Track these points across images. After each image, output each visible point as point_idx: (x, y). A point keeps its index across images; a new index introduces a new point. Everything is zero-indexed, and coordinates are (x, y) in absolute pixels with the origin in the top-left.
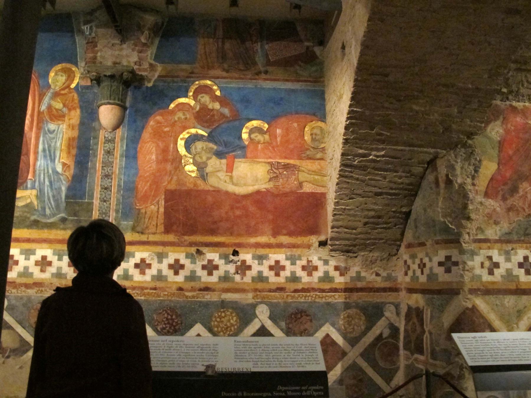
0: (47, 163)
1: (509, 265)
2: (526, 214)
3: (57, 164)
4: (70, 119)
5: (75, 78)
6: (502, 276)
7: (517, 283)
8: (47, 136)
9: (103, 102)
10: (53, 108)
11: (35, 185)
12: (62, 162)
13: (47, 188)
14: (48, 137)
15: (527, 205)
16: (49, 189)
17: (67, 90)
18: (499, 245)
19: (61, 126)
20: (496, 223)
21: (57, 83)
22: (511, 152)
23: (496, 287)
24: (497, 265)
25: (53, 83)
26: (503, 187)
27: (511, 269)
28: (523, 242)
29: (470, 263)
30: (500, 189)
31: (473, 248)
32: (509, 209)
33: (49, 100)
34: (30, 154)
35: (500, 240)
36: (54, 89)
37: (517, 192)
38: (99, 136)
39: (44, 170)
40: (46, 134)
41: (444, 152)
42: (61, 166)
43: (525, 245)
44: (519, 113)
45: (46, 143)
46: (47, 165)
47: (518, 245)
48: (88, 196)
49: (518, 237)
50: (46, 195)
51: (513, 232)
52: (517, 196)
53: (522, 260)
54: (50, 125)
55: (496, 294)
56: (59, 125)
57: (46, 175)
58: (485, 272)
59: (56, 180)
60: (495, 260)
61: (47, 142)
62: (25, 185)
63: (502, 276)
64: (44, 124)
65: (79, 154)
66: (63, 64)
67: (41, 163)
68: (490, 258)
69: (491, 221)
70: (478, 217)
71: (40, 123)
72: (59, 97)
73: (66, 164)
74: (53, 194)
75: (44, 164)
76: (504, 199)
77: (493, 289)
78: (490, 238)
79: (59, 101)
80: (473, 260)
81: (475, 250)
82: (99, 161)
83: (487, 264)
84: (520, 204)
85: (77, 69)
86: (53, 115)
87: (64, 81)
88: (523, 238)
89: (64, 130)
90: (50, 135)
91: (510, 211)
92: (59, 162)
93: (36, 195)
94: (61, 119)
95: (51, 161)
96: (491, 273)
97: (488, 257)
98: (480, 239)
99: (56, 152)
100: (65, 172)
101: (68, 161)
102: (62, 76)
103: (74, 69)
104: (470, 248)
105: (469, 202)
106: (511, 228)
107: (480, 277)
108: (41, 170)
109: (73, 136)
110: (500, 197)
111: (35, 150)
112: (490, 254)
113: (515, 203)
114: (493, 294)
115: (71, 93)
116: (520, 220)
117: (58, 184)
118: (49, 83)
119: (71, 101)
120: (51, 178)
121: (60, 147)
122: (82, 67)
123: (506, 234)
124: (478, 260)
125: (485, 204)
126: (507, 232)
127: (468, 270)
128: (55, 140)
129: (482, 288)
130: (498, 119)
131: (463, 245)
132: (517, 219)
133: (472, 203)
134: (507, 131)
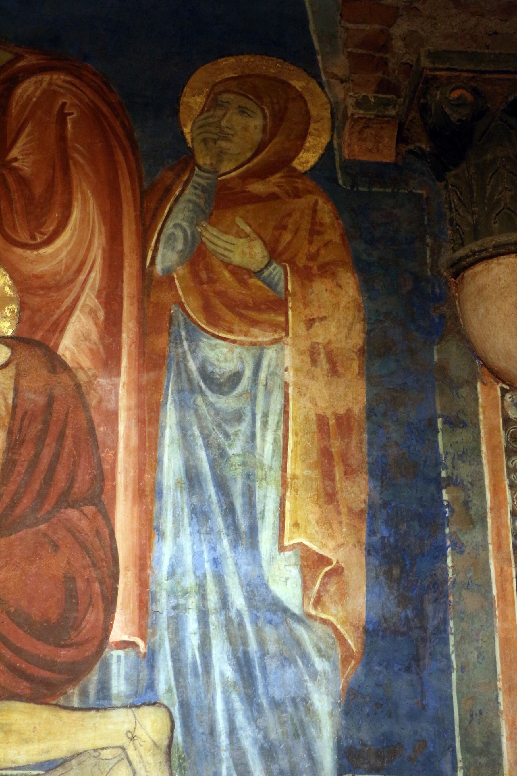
0: (214, 549)
3: (272, 559)
4: (310, 323)
5: (313, 126)
8: (199, 400)
9: (503, 238)
10: (216, 262)
11: (151, 686)
12: (293, 547)
13: (228, 701)
14: (203, 410)
16: (238, 705)
17: (276, 178)
19: (270, 353)
21: (224, 144)
25: (205, 141)
33: (194, 222)
34: (113, 499)
36: (215, 172)
38: (476, 414)
39: (201, 587)
40: (194, 389)
42: (294, 573)
45: (200, 442)
46: (216, 562)
48: (466, 748)
50: (224, 740)
54: (213, 348)
56: (261, 346)
57: (213, 619)
59: (272, 648)
61: (206, 437)
62: (94, 677)
64: (178, 341)
65: (385, 504)
66: (245, 59)
67: (179, 548)
71: (158, 331)
72: (241, 211)
73: (323, 560)
74: (266, 737)
75: (197, 555)
79: (248, 229)
82: (499, 547)
85: (313, 84)
86: (220, 294)
87: (258, 136)
89: (290, 377)
90: (212, 398)
92: (282, 548)
93: (166, 742)
94: (265, 317)
95: (234, 545)
99: (259, 493)
100: (318, 602)
101: (331, 544)
102: (243, 111)
103: (298, 84)
108: (186, 593)
109: (342, 411)
111: (141, 472)
115: (297, 194)
117: (290, 673)
118: (184, 140)
119: (304, 233)
120: (245, 642)
121: (277, 465)
122: (334, 76)
128: (244, 427)
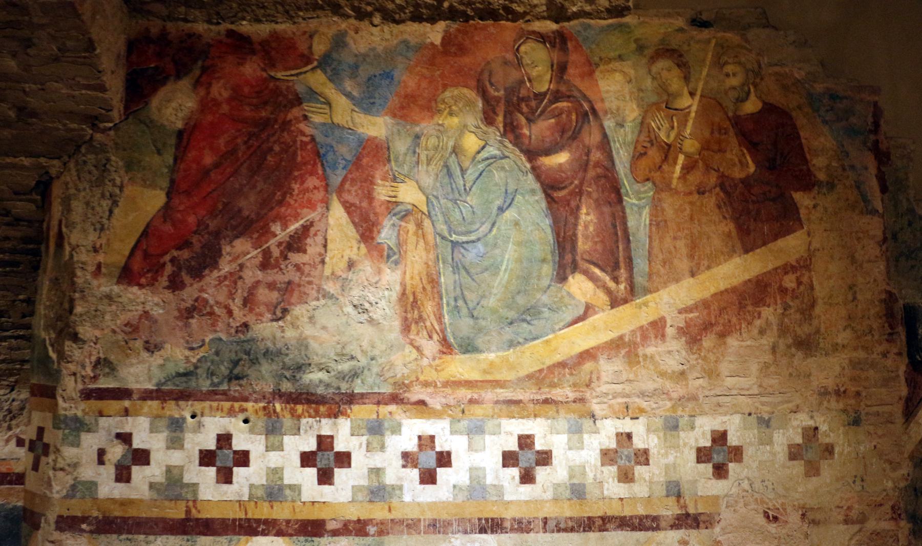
1: (176, 458)
2: (234, 324)
6: (152, 486)
7: (191, 504)
15: (238, 301)
18: (155, 404)
20: (151, 348)
22: (208, 159)
23: (132, 512)
24: (142, 457)
26: (175, 253)
27: (181, 468)
28: (226, 396)
29: (69, 452)
30: (167, 258)
31: (80, 414)
32: (188, 313)
35: (157, 391)
37: (214, 265)
41: (56, 162)
43: (227, 405)
44: (253, 52)
47: (207, 404)
49: (213, 384)
51: (199, 371)
52: (211, 277)
53: (212, 445)
55: (129, 532)
58: (108, 472)
60: (137, 444)
63: (152, 486)
68: (125, 438)
69: (139, 344)
70: (97, 333)
76: (175, 285)
77: (125, 520)
78: (133, 385)
80: (78, 445)
81: (86, 417)
83: (116, 452)
84: (222, 298)
88: (224, 387)
91: (192, 317)
96: (123, 475)
97: (119, 436)
98: (107, 390)
104: (73, 411)
105: (77, 295)
106: (194, 360)
107: (92, 486)
110: (164, 281)
112: (127, 429)
113: (206, 296)
114: (119, 532)
116: (220, 339)
123: (179, 375)
124: (90, 442)
125: (120, 300)
126: (182, 371)
127: (62, 469)
129: (95, 513)
130: (186, 74)
131: (60, 401)
132: (211, 337)
133: (83, 298)
134: (206, 105)
